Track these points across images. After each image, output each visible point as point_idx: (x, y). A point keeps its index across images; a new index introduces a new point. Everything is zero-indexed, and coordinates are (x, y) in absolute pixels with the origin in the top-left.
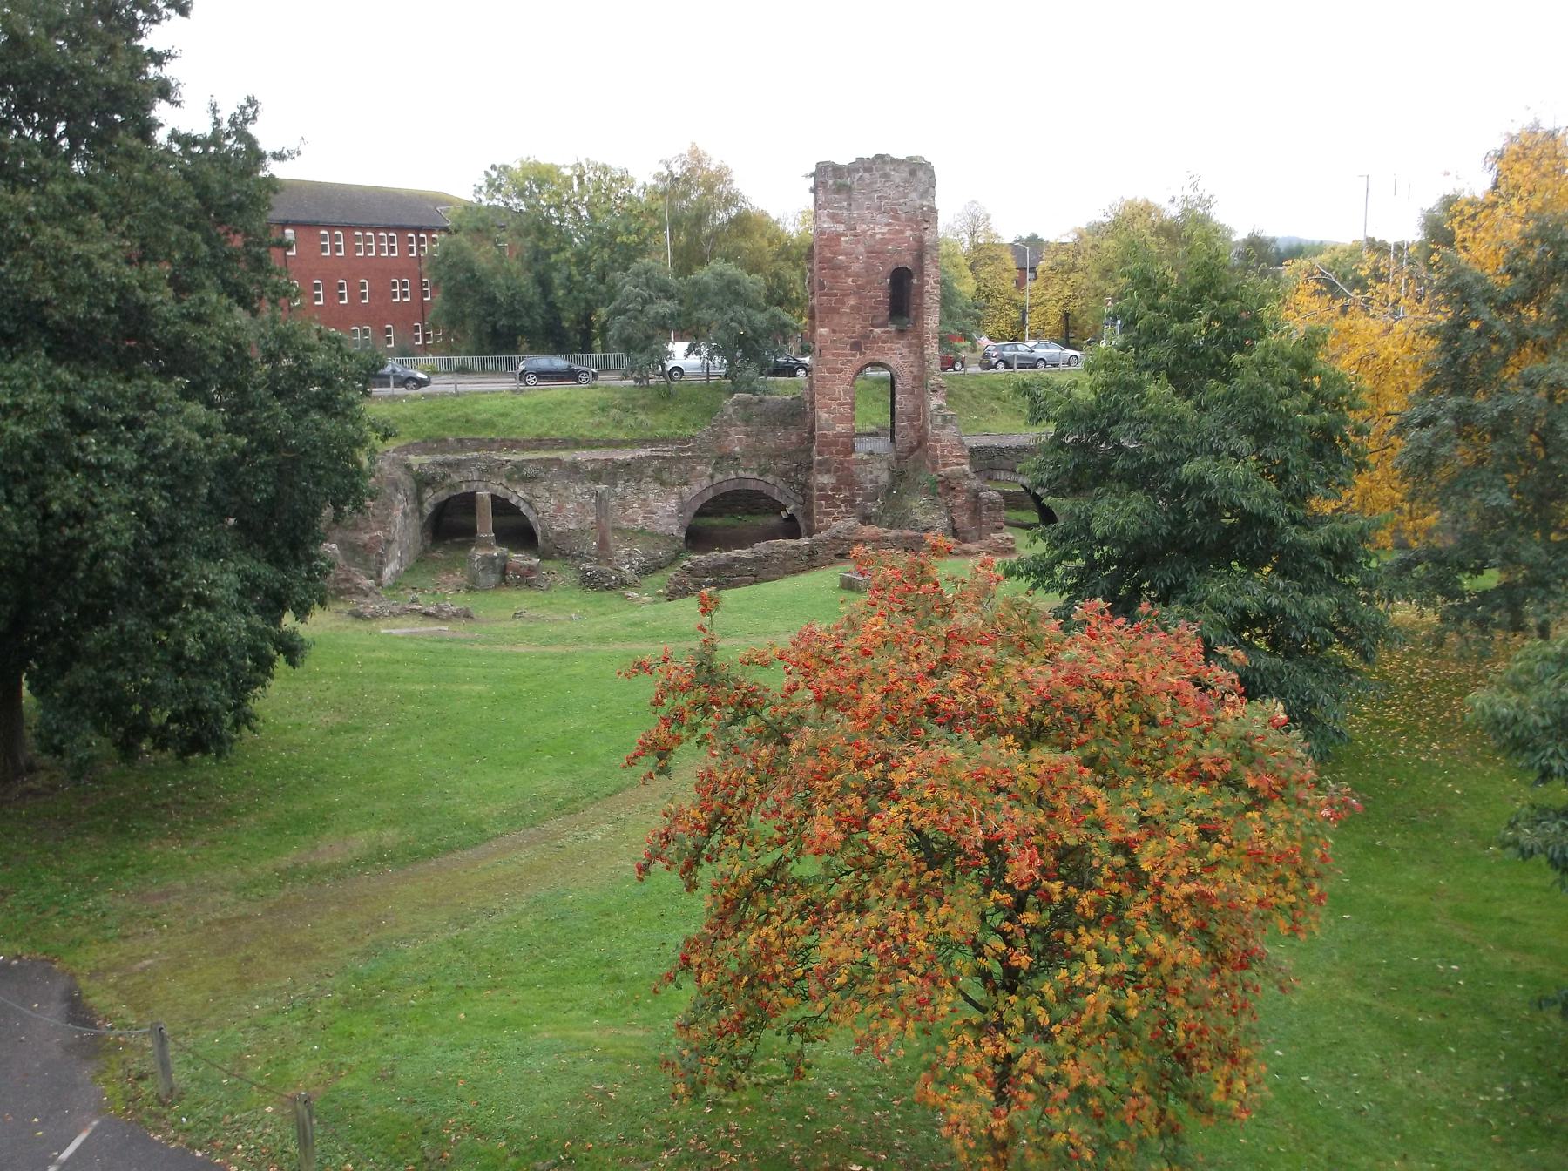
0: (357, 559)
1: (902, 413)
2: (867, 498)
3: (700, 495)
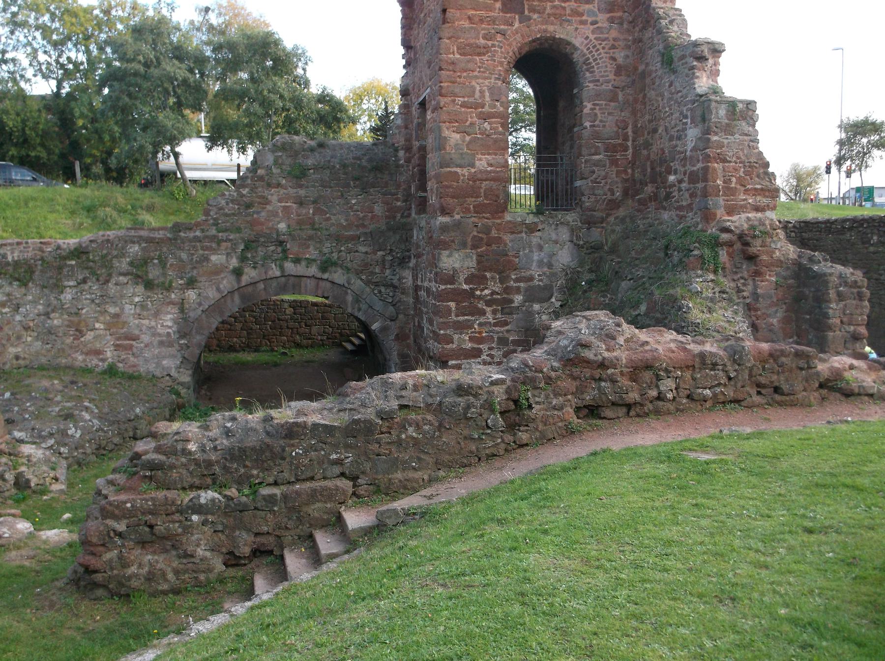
1: (596, 136)
2: (532, 296)
3: (217, 307)
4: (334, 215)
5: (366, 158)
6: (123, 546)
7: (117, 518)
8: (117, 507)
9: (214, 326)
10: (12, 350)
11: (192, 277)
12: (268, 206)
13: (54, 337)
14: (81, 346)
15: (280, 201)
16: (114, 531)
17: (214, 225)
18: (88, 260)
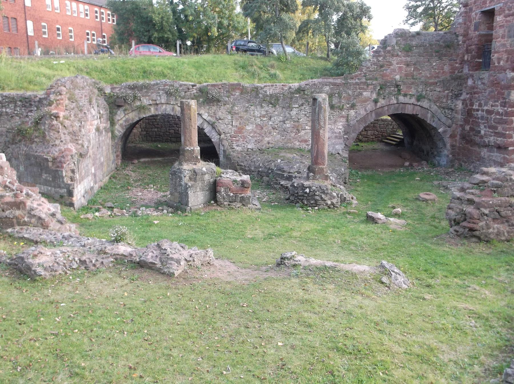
0: (44, 176)
3: (364, 119)
4: (424, 71)
5: (442, 40)
6: (488, 220)
7: (485, 208)
8: (486, 203)
9: (361, 129)
10: (267, 139)
11: (353, 103)
12: (391, 67)
13: (286, 133)
14: (298, 138)
15: (397, 64)
16: (484, 213)
17: (365, 76)
18: (304, 93)
